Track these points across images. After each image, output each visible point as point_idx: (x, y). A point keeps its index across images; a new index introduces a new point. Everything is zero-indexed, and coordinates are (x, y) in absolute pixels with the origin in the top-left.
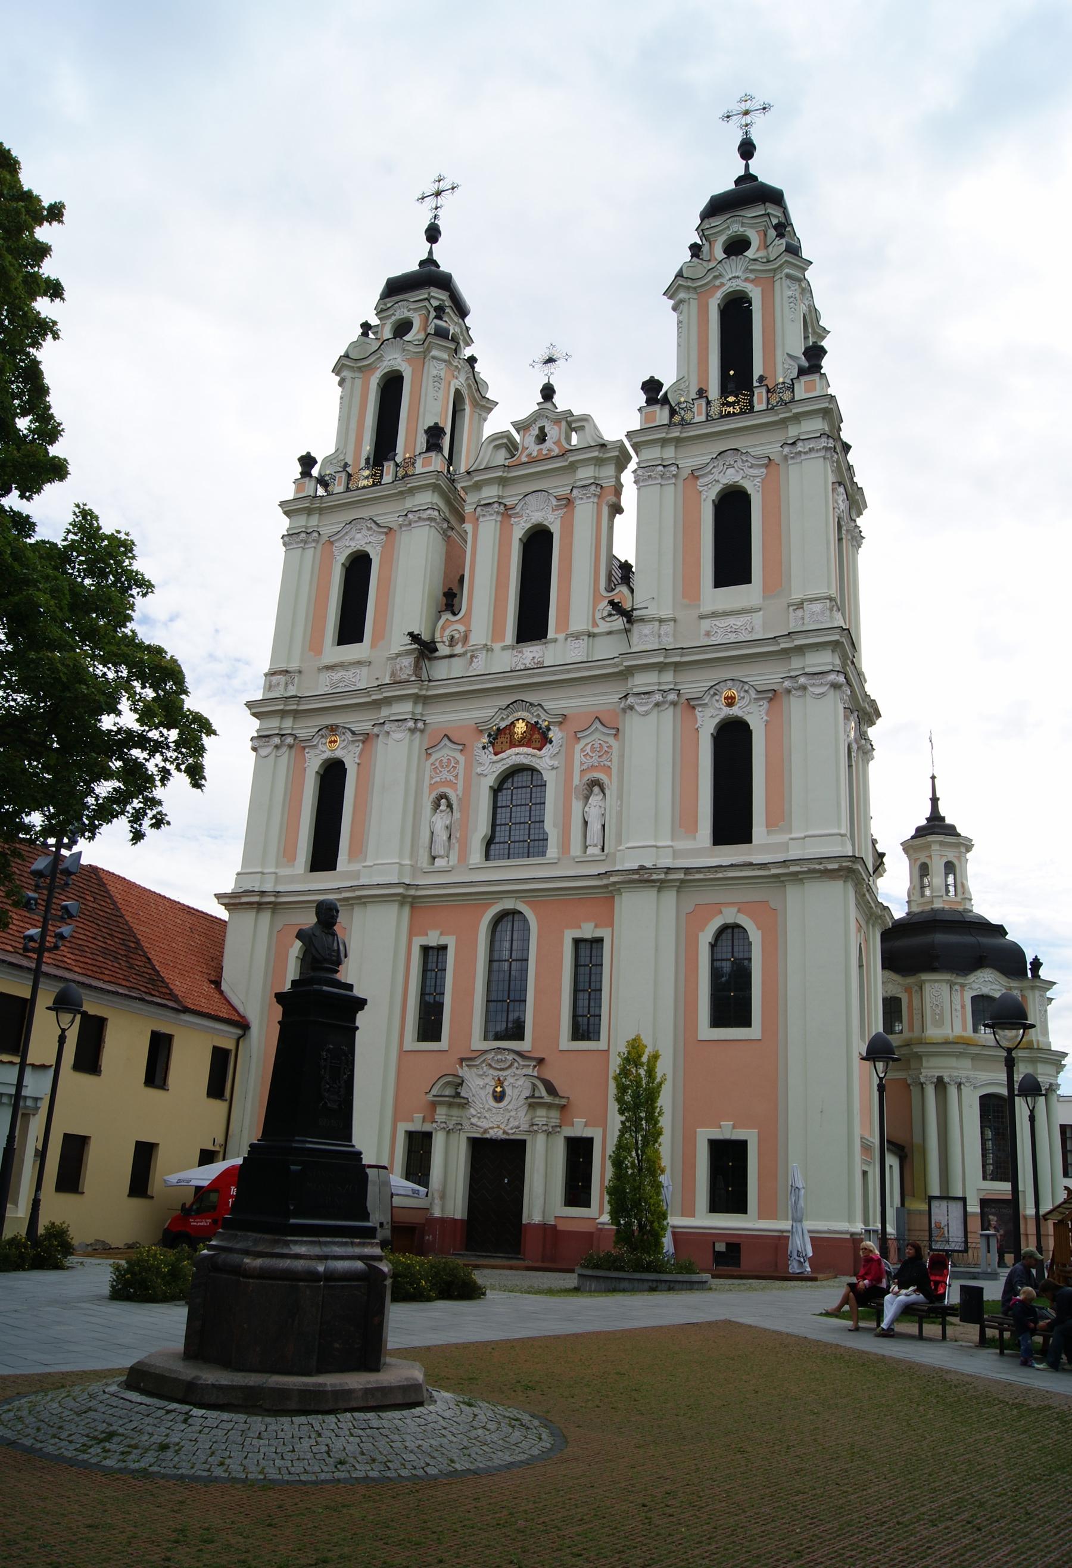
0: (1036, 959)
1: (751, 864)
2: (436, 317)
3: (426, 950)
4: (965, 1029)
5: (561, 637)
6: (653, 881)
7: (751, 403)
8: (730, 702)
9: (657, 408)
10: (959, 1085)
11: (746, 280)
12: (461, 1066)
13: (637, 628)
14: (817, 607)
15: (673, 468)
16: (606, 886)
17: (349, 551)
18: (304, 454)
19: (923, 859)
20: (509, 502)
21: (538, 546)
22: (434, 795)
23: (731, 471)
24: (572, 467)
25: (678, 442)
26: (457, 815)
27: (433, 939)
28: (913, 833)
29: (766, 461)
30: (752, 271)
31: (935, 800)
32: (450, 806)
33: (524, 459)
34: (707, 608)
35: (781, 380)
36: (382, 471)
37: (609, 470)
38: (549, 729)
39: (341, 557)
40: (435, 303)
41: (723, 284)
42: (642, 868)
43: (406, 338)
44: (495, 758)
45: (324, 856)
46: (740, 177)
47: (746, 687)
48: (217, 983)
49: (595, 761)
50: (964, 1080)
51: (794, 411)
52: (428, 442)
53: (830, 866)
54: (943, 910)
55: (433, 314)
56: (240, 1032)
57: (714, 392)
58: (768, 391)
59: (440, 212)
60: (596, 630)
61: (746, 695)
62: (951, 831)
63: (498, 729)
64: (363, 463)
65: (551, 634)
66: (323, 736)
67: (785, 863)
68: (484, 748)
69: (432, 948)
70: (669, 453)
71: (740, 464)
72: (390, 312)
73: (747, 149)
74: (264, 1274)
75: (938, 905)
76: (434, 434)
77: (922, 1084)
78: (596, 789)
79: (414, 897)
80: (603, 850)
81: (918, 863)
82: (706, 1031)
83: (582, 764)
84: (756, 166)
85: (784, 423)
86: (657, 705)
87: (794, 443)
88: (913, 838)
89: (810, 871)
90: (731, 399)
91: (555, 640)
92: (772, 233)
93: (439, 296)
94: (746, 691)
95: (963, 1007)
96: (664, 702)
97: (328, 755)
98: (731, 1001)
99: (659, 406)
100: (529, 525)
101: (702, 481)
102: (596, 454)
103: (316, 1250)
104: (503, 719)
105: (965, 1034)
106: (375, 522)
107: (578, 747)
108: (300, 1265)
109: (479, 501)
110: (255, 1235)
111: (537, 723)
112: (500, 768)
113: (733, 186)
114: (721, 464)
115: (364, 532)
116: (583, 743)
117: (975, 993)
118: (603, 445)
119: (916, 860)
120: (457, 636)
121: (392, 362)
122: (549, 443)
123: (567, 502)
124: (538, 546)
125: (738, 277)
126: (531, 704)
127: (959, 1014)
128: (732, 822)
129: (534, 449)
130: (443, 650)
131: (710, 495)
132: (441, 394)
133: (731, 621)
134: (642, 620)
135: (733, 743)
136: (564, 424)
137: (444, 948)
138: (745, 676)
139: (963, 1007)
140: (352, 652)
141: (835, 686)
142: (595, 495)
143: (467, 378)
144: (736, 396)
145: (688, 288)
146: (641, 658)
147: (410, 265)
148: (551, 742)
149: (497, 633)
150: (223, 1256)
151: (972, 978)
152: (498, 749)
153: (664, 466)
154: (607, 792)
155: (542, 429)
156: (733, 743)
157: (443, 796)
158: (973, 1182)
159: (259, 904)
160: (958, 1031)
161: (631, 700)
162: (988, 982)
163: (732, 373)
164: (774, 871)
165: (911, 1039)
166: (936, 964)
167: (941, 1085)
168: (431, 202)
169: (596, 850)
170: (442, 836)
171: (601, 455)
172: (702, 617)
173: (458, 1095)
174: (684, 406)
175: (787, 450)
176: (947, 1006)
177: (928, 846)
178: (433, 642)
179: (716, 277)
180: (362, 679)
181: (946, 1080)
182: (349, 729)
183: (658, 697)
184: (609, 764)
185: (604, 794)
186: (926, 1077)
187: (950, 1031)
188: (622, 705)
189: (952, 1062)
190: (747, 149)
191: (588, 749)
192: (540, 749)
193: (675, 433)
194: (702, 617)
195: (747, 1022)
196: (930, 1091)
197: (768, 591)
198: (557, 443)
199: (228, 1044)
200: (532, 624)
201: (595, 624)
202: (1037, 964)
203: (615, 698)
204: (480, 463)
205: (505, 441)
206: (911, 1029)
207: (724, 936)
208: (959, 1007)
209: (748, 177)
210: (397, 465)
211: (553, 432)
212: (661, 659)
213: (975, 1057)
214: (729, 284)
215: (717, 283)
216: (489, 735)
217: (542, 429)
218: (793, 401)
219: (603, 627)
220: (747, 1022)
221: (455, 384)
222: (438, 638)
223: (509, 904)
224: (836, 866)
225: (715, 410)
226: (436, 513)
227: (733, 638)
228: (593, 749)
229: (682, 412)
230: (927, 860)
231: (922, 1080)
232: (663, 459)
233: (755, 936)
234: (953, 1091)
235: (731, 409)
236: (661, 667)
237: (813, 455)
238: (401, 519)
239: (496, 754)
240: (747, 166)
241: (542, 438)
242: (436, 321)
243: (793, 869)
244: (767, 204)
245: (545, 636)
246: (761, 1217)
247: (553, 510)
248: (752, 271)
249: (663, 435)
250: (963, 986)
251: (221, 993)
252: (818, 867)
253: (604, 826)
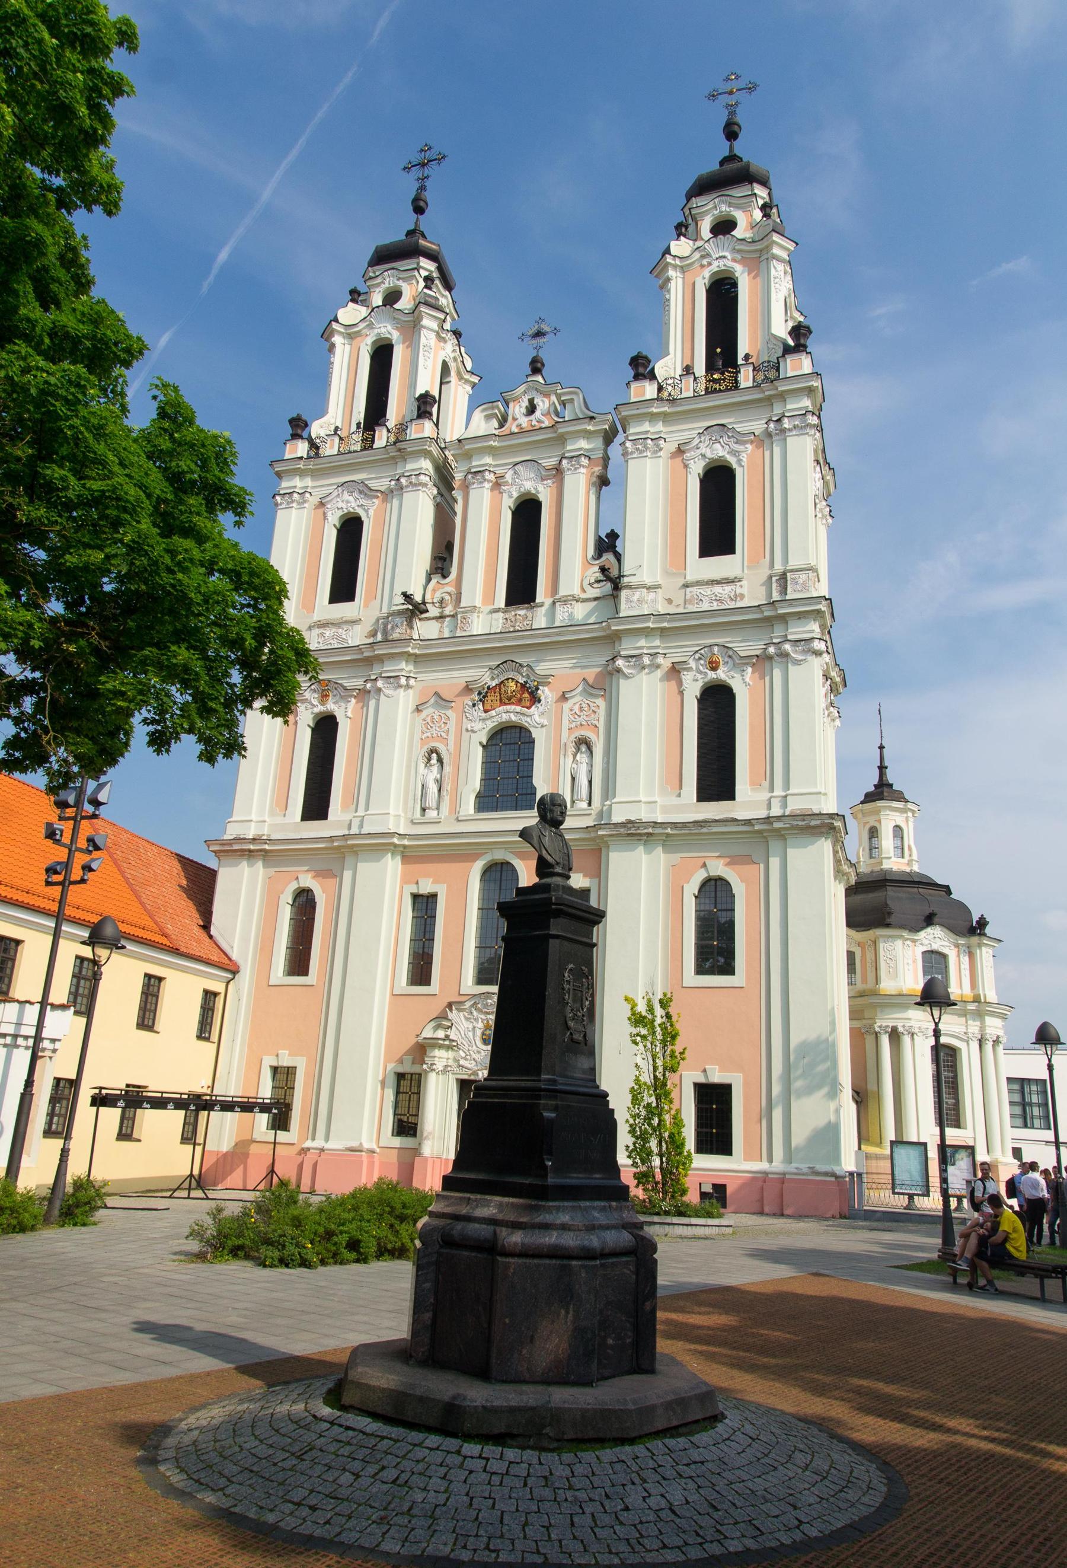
0: (982, 918)
1: (735, 820)
2: (426, 287)
3: (416, 897)
5: (548, 602)
6: (640, 835)
7: (736, 381)
8: (714, 668)
10: (913, 1035)
11: (734, 260)
12: (451, 1010)
13: (624, 594)
14: (802, 577)
16: (593, 839)
17: (340, 513)
18: (295, 415)
19: (872, 823)
20: (499, 471)
21: (527, 515)
22: (425, 749)
25: (665, 417)
26: (447, 769)
27: (426, 887)
28: (862, 798)
30: (739, 251)
31: (882, 768)
32: (440, 760)
33: (515, 429)
34: (690, 578)
35: (766, 359)
36: (374, 436)
37: (599, 443)
38: (537, 689)
39: (334, 519)
40: (424, 273)
41: (710, 264)
42: (630, 822)
43: (396, 306)
44: (484, 715)
45: (316, 805)
46: (725, 158)
47: (730, 653)
48: (206, 927)
49: (582, 720)
50: (916, 1030)
52: (419, 408)
53: (813, 823)
54: (890, 871)
55: (422, 284)
56: (230, 976)
57: (700, 369)
59: (428, 183)
60: (583, 596)
61: (729, 660)
62: (899, 797)
63: (489, 688)
64: (354, 428)
65: (540, 596)
66: (314, 691)
67: (768, 820)
68: (474, 705)
69: (422, 895)
71: (726, 438)
72: (379, 280)
73: (731, 133)
74: (525, 1253)
75: (886, 865)
76: (425, 405)
77: (876, 1034)
78: (583, 748)
79: (405, 847)
80: (590, 804)
81: (868, 827)
82: (690, 977)
83: (571, 722)
84: (740, 147)
85: (769, 401)
87: (779, 420)
88: (862, 803)
89: (793, 827)
91: (542, 605)
92: (758, 215)
93: (428, 266)
94: (730, 657)
95: (914, 961)
97: (319, 709)
98: (716, 950)
103: (579, 1220)
104: (493, 679)
106: (366, 485)
107: (567, 706)
108: (570, 1240)
109: (470, 469)
110: (498, 1198)
111: (526, 683)
112: (491, 724)
113: (717, 167)
114: (708, 437)
115: (356, 494)
116: (570, 702)
117: (925, 949)
118: (592, 418)
119: (865, 823)
120: (447, 597)
121: (383, 330)
122: (538, 413)
123: (558, 472)
124: (527, 515)
125: (725, 257)
126: (520, 665)
127: (911, 967)
128: (717, 778)
129: (524, 421)
130: (434, 611)
131: (697, 468)
132: (430, 363)
133: (718, 589)
134: (629, 587)
135: (717, 704)
136: (554, 398)
137: (434, 896)
139: (914, 961)
140: (344, 610)
141: (818, 653)
143: (454, 351)
144: (723, 373)
145: (675, 267)
146: (629, 624)
147: (396, 235)
148: (539, 701)
149: (489, 596)
150: (459, 1226)
151: (922, 934)
152: (488, 707)
154: (594, 749)
155: (531, 401)
156: (717, 704)
157: (433, 750)
158: (923, 1127)
159: (250, 851)
161: (620, 663)
162: (935, 938)
163: (718, 350)
164: (757, 828)
165: (864, 991)
166: (888, 921)
167: (895, 1035)
168: (416, 173)
169: (584, 805)
170: (433, 788)
172: (686, 586)
173: (447, 1037)
174: (670, 381)
176: (902, 960)
177: (877, 812)
178: (424, 603)
179: (703, 257)
180: (356, 637)
181: (900, 1029)
182: (341, 684)
184: (596, 723)
185: (591, 753)
186: (880, 1027)
188: (610, 668)
190: (731, 133)
191: (576, 709)
192: (529, 708)
194: (686, 586)
195: (728, 969)
196: (885, 1040)
197: (754, 563)
198: (547, 414)
199: (218, 987)
200: (521, 588)
201: (584, 591)
202: (982, 923)
203: (603, 660)
206: (864, 980)
207: (707, 888)
208: (910, 962)
209: (732, 158)
210: (388, 431)
211: (542, 404)
214: (716, 263)
215: (705, 262)
216: (479, 694)
217: (531, 401)
218: (778, 378)
219: (593, 592)
220: (728, 969)
221: (441, 356)
222: (428, 599)
223: (499, 855)
224: (818, 822)
225: (701, 387)
226: (428, 478)
227: (715, 606)
228: (581, 709)
230: (876, 824)
231: (877, 1029)
233: (739, 889)
234: (906, 1040)
235: (717, 386)
236: (647, 632)
238: (393, 483)
239: (486, 711)
240: (731, 147)
241: (531, 409)
242: (426, 291)
243: (777, 825)
244: (755, 185)
245: (534, 600)
246: (748, 1158)
248: (739, 251)
251: (211, 937)
252: (800, 823)
253: (590, 782)
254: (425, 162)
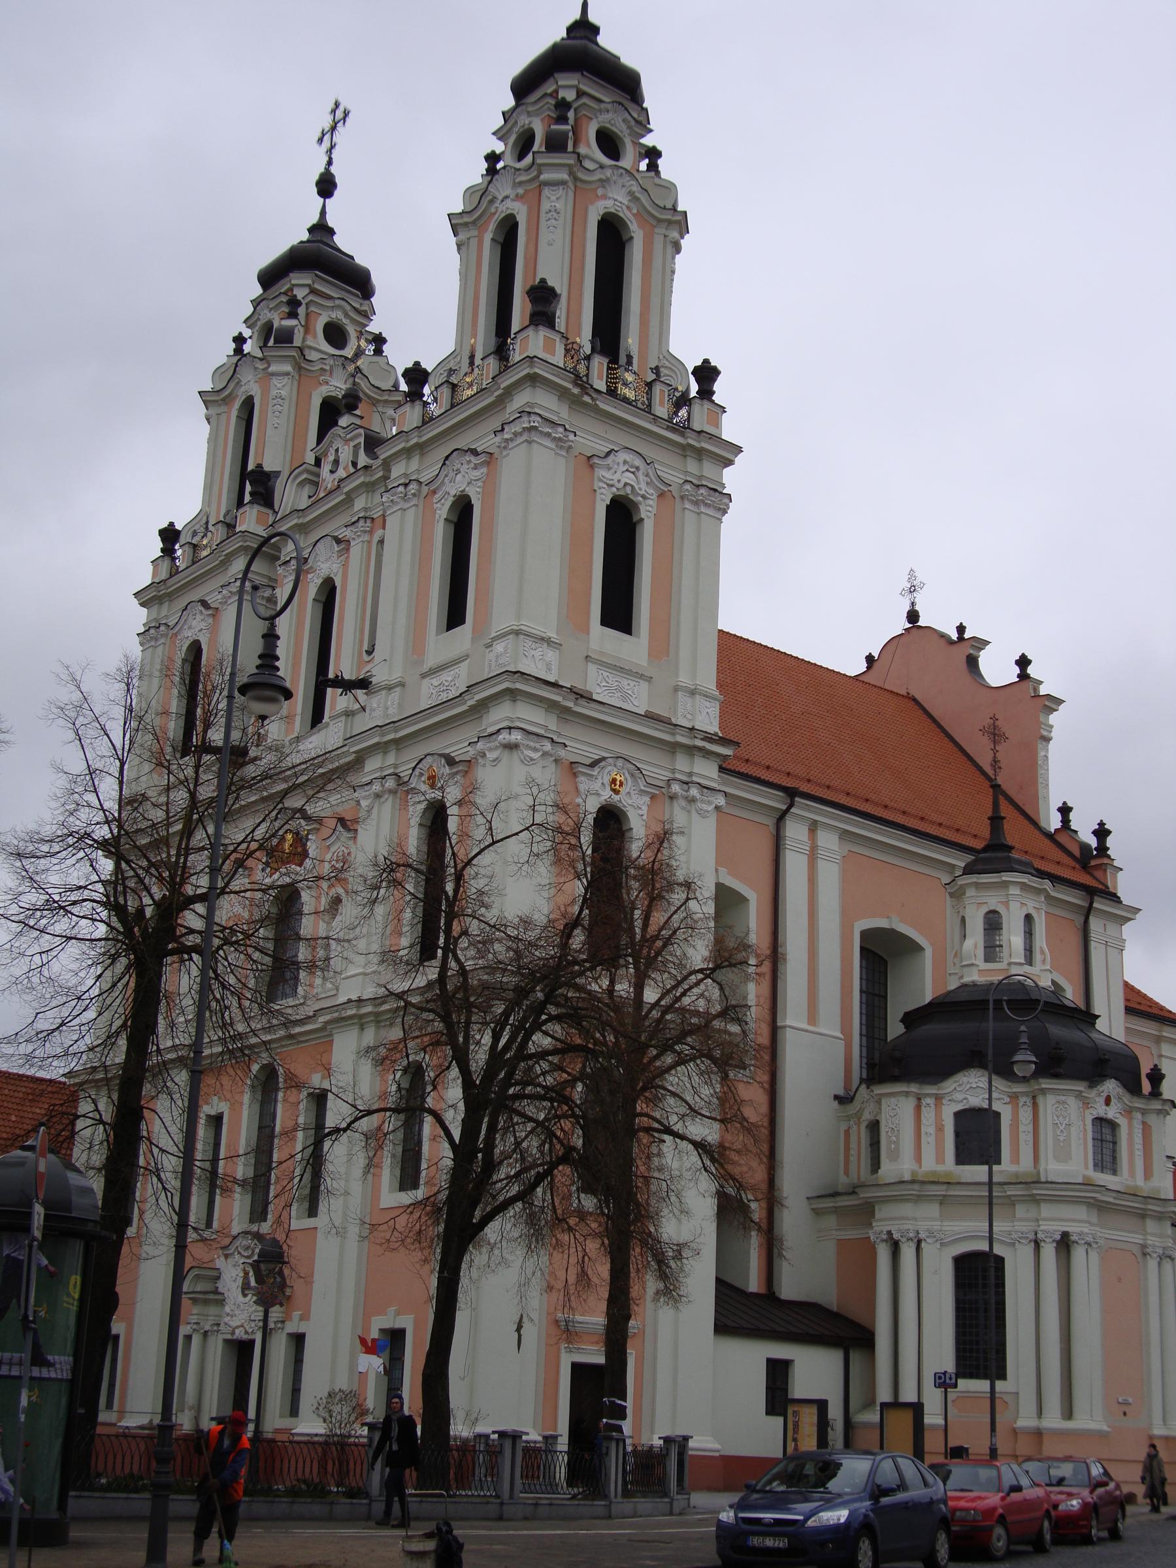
4: (940, 1159)
11: (518, 197)
24: (349, 499)
86: (378, 796)
95: (940, 1129)
96: (383, 792)
100: (321, 580)
102: (361, 479)
105: (940, 1168)
117: (960, 1107)
127: (932, 1139)
138: (446, 747)
139: (940, 1129)
142: (365, 532)
145: (466, 224)
151: (949, 1085)
160: (929, 1164)
171: (367, 480)
183: (376, 787)
187: (915, 1167)
189: (907, 1209)
197: (477, 633)
204: (285, 510)
205: (304, 476)
208: (932, 1130)
212: (376, 740)
213: (943, 1201)
247: (339, 557)
248: (521, 183)
250: (938, 1098)
254: (339, 116)
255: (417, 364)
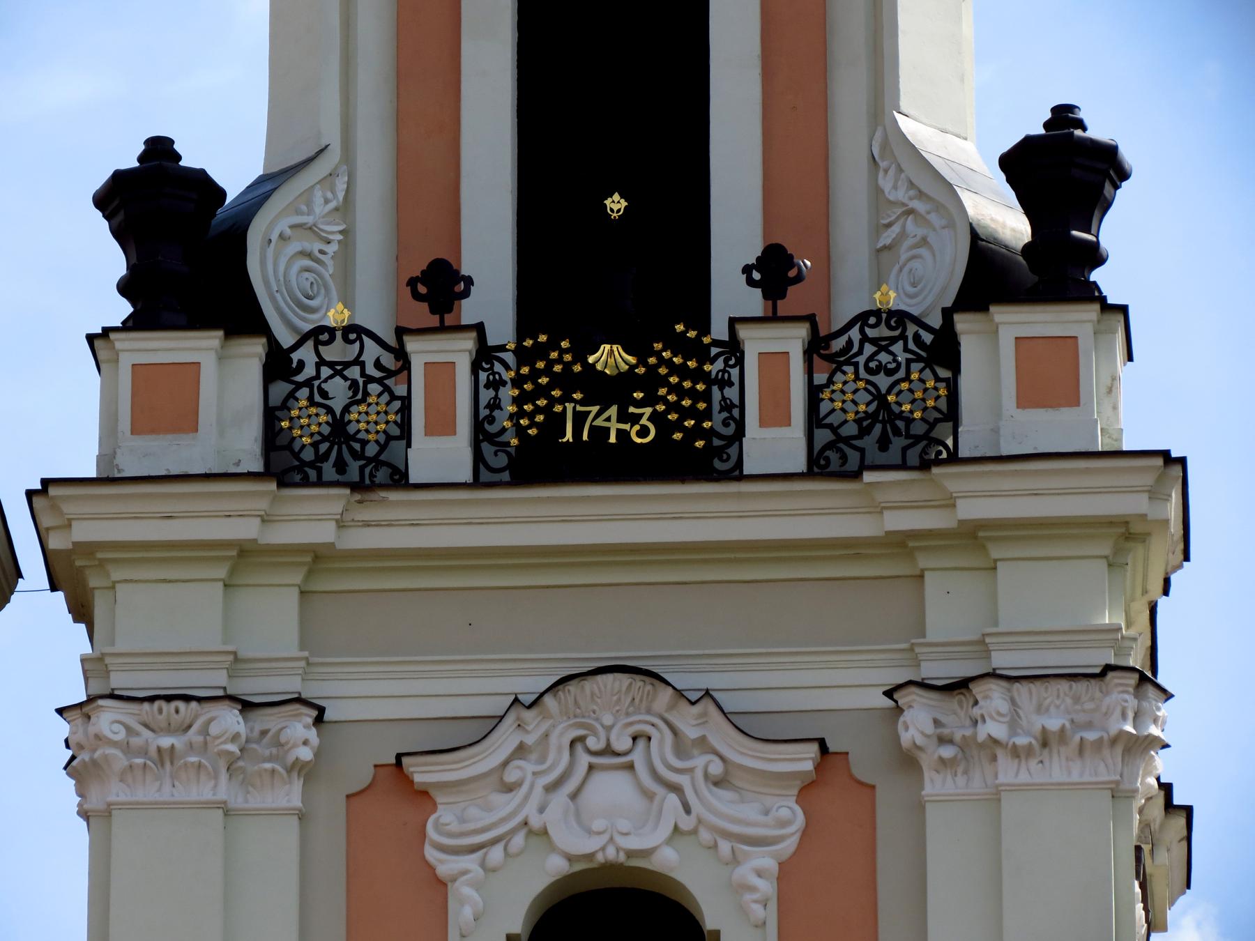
9: (198, 348)
15: (298, 731)
23: (611, 789)
29: (804, 760)
51: (970, 510)
58: (816, 347)
70: (271, 620)
71: (662, 744)
90: (610, 358)
99: (213, 339)
101: (446, 819)
114: (562, 735)
144: (637, 348)
153: (247, 706)
174: (336, 351)
175: (919, 718)
193: (314, 516)
229: (338, 390)
232: (237, 662)
237: (1058, 769)
249: (247, 530)
255: (159, 151)
